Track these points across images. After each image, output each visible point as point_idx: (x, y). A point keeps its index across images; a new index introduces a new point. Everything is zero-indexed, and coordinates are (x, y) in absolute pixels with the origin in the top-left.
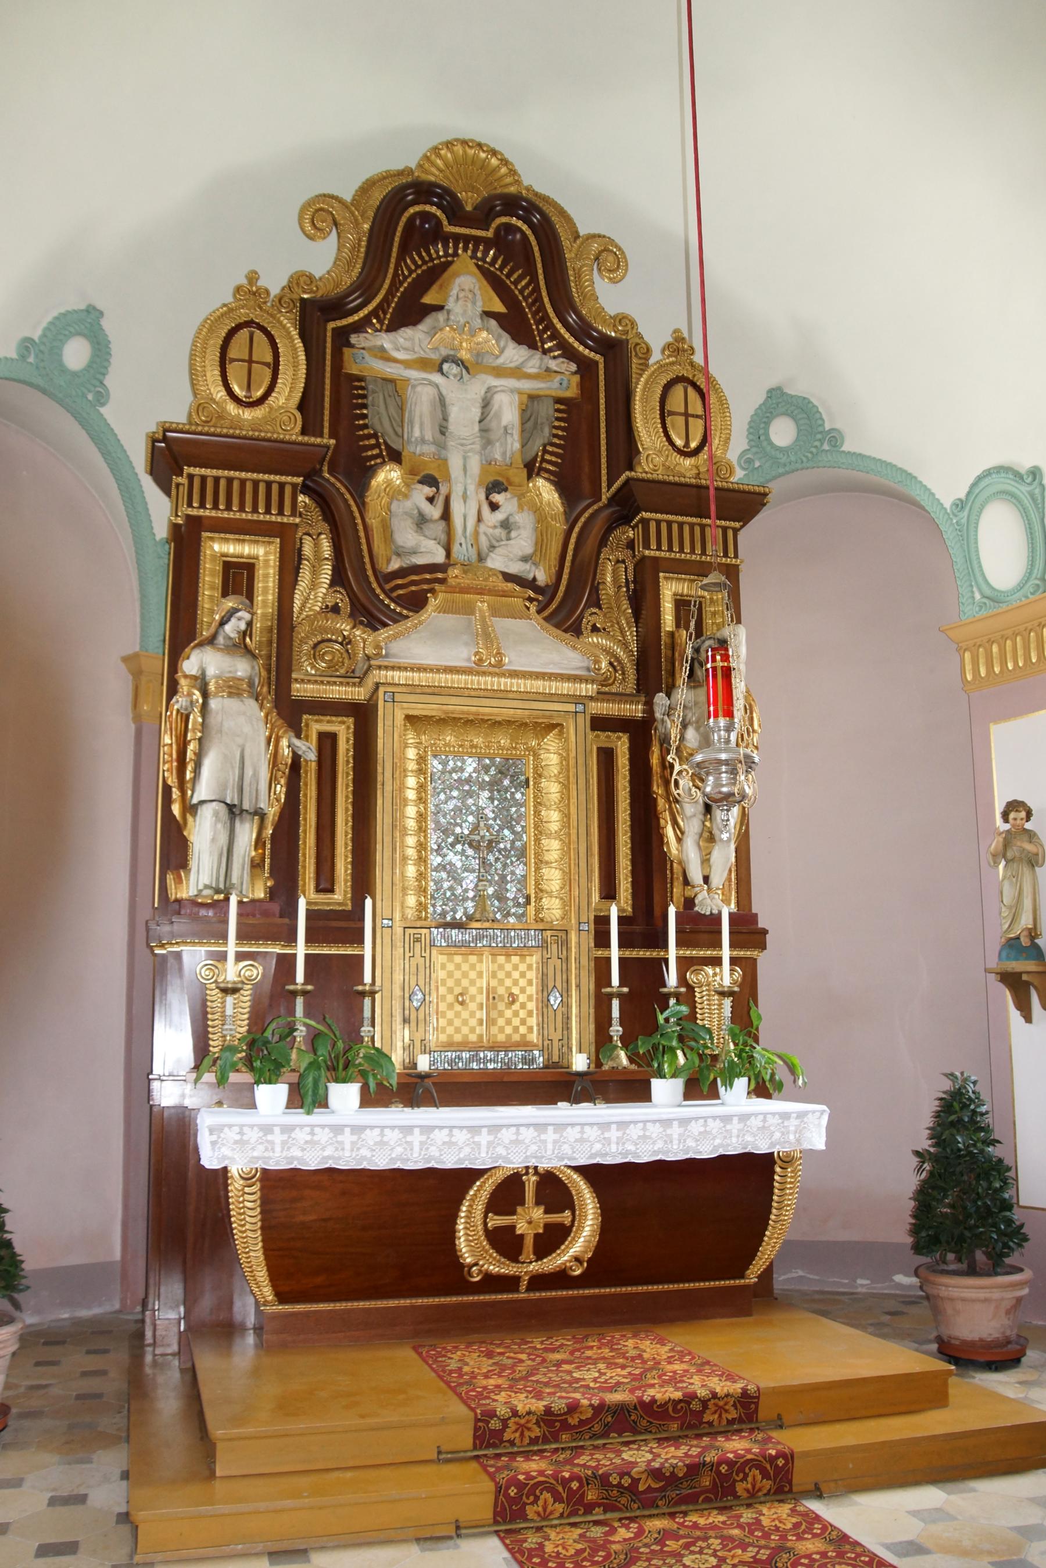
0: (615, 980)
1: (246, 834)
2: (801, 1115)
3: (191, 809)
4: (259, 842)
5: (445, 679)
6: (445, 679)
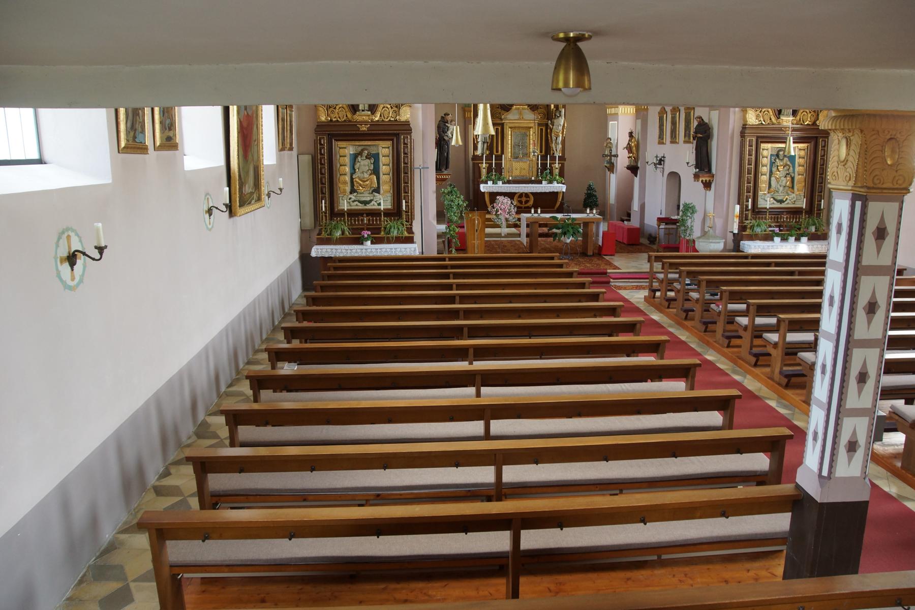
0: (539, 166)
1: (486, 145)
2: (562, 187)
3: (478, 142)
4: (487, 146)
5: (515, 121)
6: (515, 121)
